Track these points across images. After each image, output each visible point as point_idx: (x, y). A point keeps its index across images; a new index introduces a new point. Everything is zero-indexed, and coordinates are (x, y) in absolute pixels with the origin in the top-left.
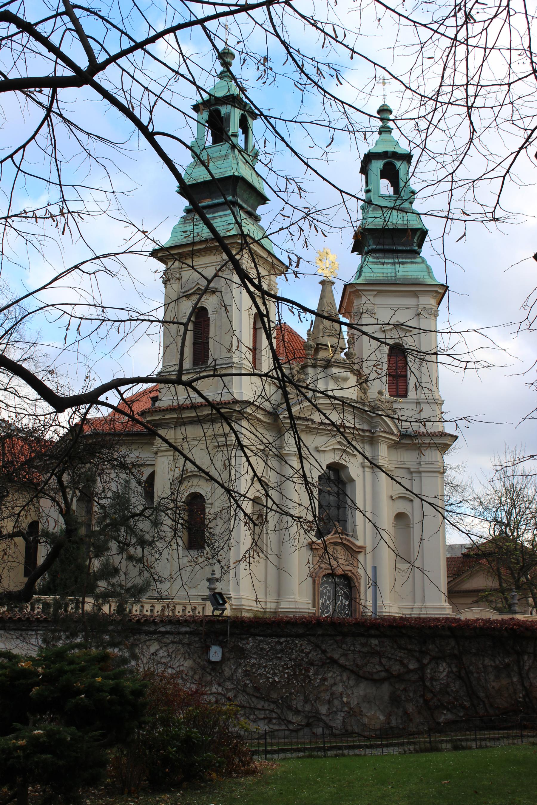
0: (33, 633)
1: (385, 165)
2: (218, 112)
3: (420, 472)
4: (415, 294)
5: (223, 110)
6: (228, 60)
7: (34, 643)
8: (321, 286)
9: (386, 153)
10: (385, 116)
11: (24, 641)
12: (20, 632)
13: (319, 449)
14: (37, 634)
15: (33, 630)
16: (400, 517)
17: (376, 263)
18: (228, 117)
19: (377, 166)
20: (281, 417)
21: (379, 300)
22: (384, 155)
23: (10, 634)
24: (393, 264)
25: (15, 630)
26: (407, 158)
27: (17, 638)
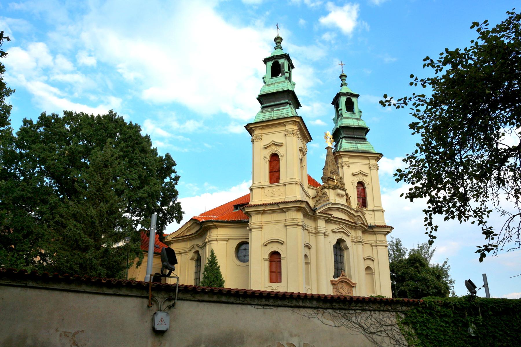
0: (353, 312)
1: (347, 99)
2: (278, 62)
3: (376, 246)
4: (368, 158)
5: (281, 61)
6: (279, 41)
7: (355, 321)
8: (326, 150)
9: (347, 93)
10: (344, 78)
11: (348, 319)
12: (343, 311)
13: (334, 230)
14: (355, 313)
15: (352, 310)
16: (368, 268)
17: (348, 143)
18: (283, 64)
19: (343, 99)
20: (317, 212)
21: (351, 160)
22: (347, 94)
23: (337, 313)
24: (356, 143)
25: (340, 309)
26: (357, 96)
27: (342, 316)
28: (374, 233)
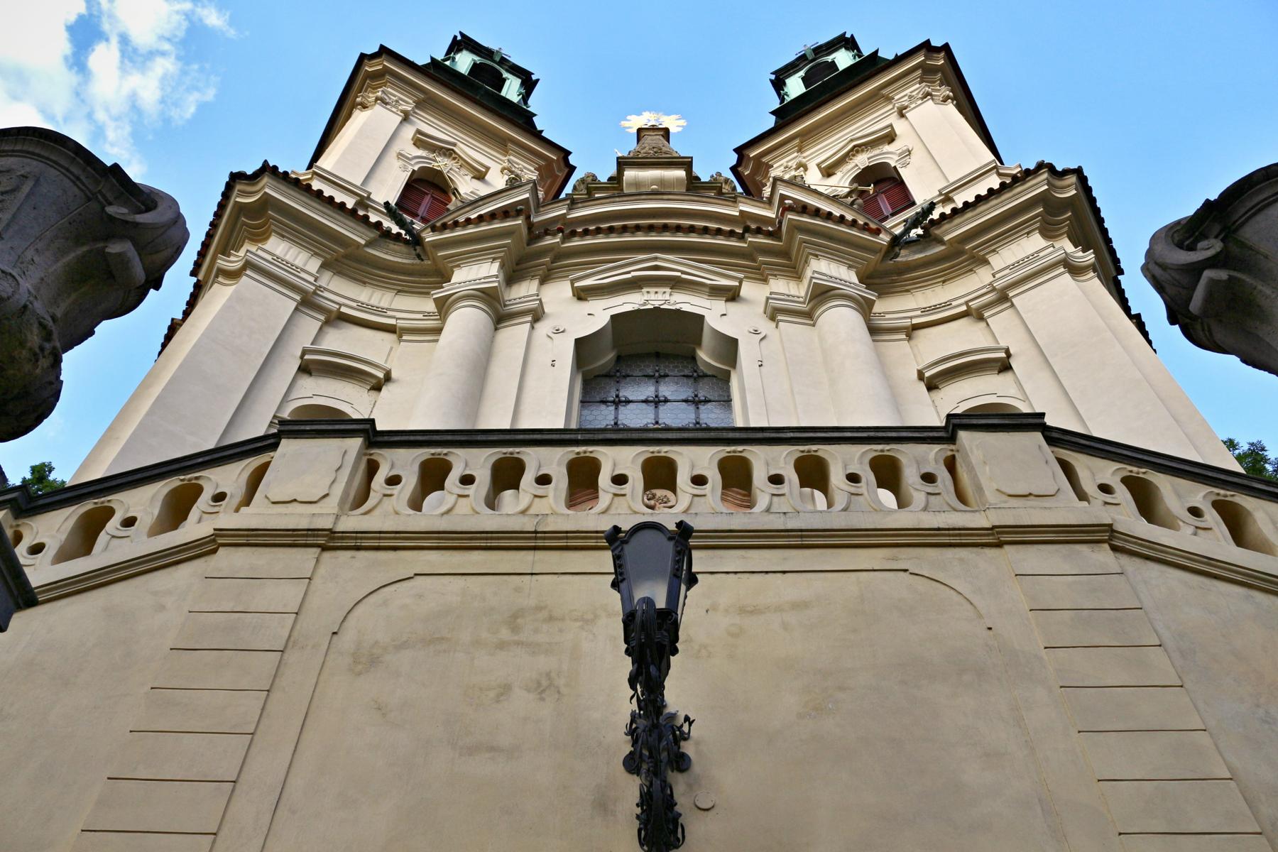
28: (965, 256)
